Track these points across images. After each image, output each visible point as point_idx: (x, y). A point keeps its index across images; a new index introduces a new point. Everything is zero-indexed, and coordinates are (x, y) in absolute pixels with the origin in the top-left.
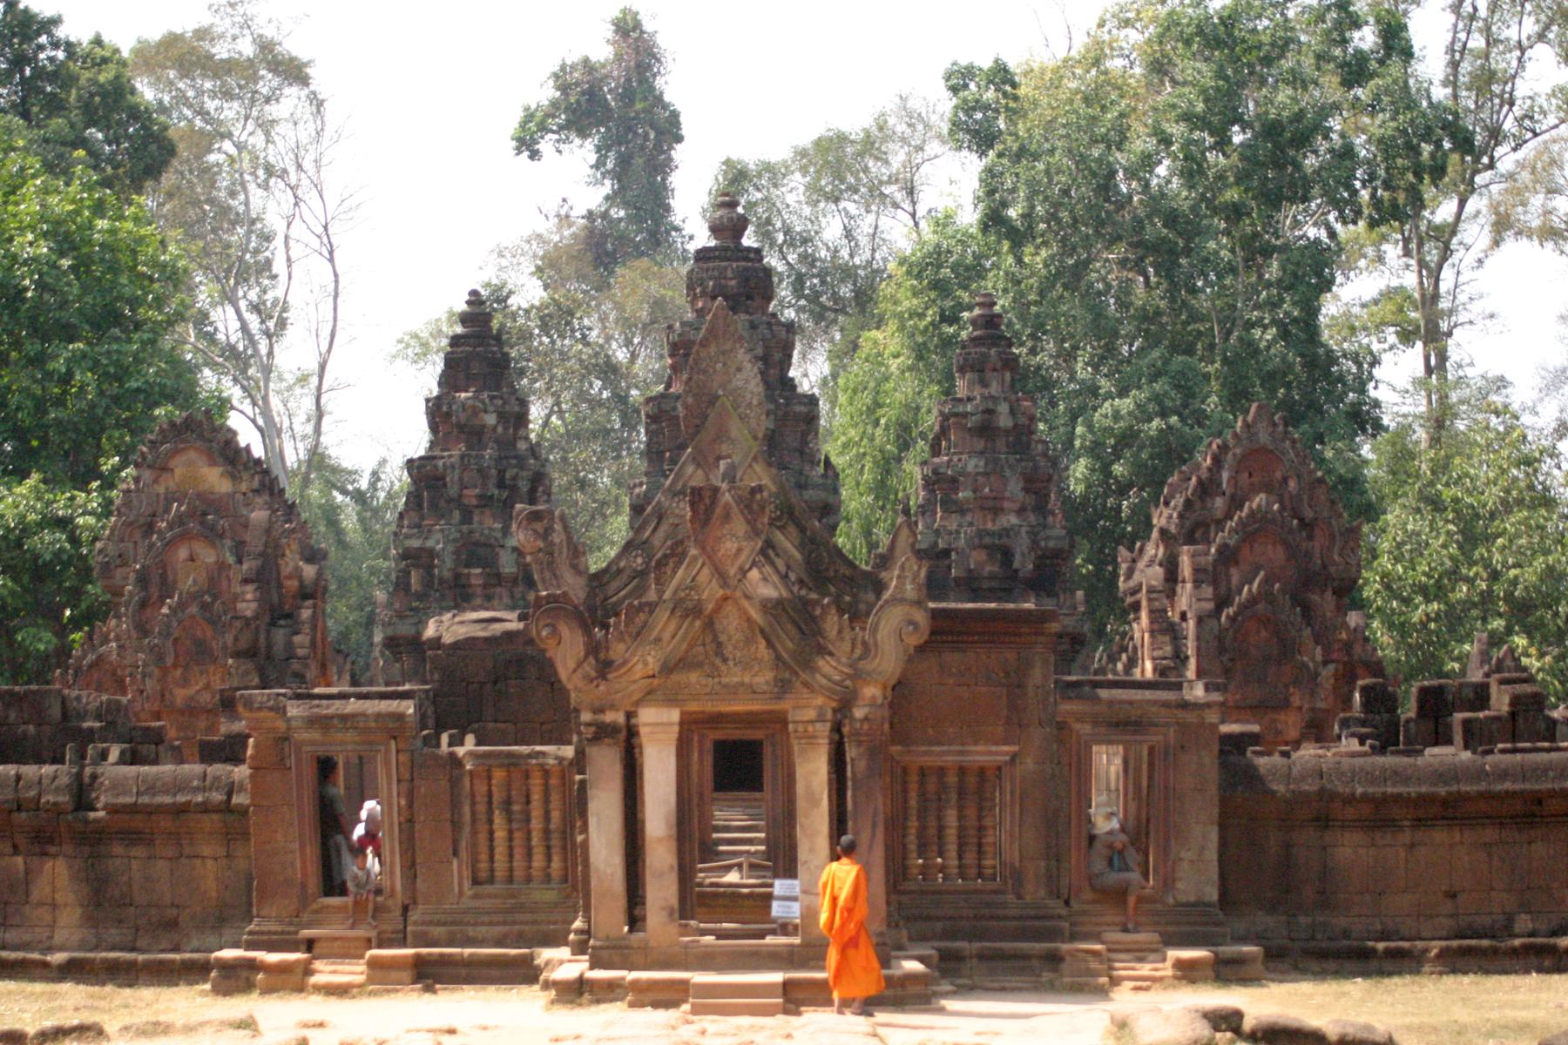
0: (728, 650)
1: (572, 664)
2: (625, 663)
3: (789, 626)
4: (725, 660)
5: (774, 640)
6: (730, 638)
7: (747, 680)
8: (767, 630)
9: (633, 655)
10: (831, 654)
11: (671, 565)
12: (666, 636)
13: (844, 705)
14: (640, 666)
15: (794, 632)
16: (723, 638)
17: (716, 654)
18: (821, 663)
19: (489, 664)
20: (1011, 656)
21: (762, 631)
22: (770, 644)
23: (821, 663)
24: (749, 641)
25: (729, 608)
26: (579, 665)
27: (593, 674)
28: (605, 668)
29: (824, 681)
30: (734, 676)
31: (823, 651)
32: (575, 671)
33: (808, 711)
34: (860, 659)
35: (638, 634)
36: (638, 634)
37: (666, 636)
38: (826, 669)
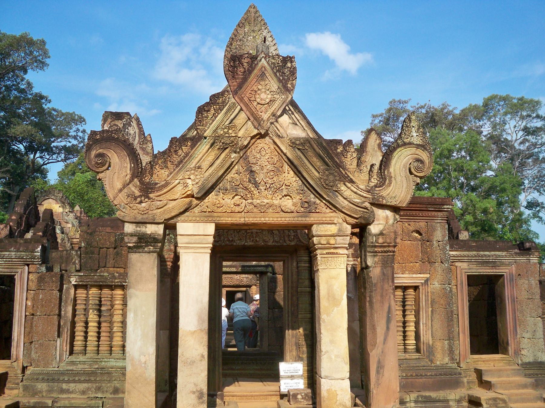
1: (119, 185)
2: (167, 184)
3: (315, 159)
4: (256, 185)
5: (301, 169)
6: (262, 168)
7: (276, 202)
8: (296, 162)
10: (352, 181)
11: (212, 111)
12: (205, 165)
15: (318, 163)
16: (255, 168)
17: (250, 181)
18: (343, 188)
19: (113, 239)
20: (421, 225)
21: (291, 163)
22: (298, 173)
23: (343, 188)
24: (278, 171)
27: (137, 193)
28: (147, 189)
29: (346, 203)
30: (263, 198)
32: (121, 190)
33: (331, 230)
34: (376, 186)
35: (181, 161)
36: (181, 161)
37: (205, 165)
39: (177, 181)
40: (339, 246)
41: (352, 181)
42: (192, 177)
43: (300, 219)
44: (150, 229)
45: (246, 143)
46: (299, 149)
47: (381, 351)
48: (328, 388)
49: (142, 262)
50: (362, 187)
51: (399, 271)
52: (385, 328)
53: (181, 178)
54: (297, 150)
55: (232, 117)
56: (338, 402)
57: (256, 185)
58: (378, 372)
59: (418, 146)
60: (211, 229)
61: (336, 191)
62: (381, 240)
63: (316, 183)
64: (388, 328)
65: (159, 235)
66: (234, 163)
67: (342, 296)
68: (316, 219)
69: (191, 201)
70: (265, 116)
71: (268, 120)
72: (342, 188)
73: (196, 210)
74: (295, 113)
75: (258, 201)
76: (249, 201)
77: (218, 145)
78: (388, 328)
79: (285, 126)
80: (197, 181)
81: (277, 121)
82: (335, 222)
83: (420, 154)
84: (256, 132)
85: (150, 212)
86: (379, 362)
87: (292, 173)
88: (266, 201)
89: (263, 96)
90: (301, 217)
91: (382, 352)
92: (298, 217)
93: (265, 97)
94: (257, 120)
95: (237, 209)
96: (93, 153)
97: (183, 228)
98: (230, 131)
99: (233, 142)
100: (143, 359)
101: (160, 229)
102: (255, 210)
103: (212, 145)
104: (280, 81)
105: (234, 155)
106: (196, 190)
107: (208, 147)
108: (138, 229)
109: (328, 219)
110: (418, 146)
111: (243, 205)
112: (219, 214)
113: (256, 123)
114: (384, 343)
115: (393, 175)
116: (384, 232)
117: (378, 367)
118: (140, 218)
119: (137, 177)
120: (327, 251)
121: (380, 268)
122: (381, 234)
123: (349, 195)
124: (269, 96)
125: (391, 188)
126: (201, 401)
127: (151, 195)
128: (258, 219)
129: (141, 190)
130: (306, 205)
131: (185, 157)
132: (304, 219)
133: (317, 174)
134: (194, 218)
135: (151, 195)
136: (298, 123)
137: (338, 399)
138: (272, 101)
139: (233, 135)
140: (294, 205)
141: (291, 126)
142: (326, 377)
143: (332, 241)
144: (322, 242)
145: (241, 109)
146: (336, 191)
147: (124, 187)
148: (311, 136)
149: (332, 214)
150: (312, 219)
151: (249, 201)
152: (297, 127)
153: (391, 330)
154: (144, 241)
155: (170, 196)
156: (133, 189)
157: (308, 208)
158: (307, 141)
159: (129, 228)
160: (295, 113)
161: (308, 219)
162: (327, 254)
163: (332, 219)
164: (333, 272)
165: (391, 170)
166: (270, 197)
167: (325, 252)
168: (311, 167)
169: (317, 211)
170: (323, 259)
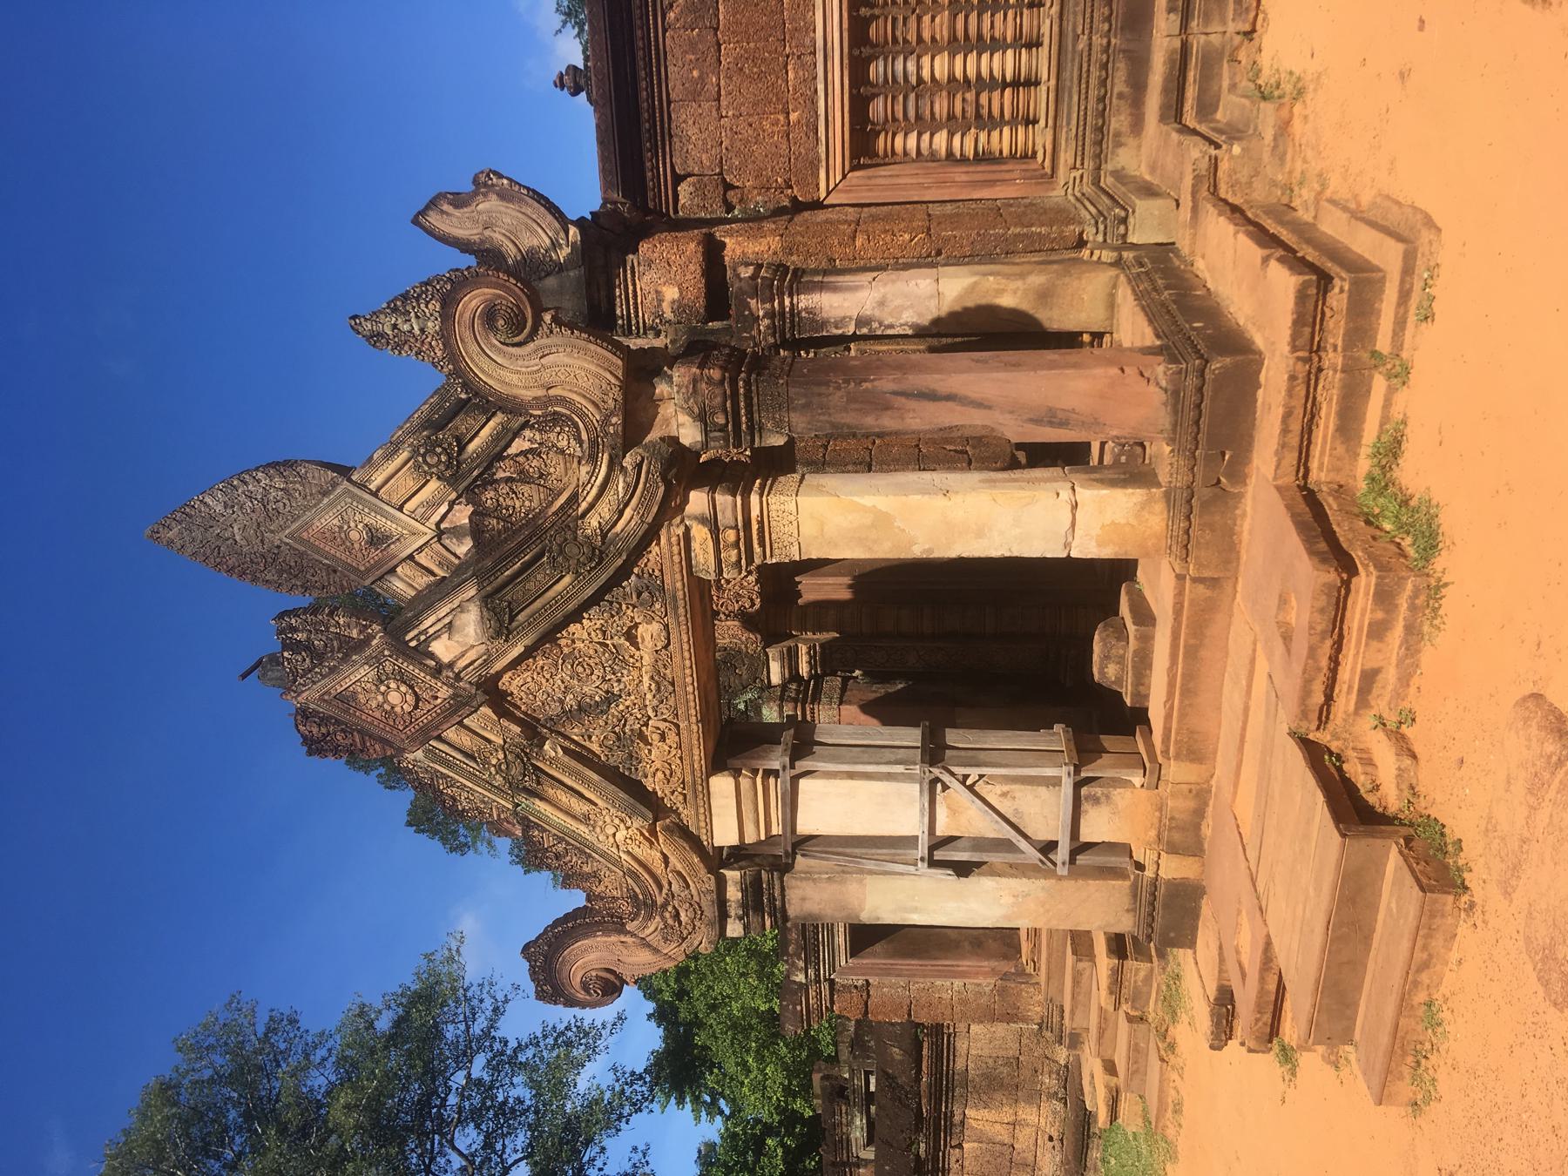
0: (592, 689)
3: (531, 585)
4: (610, 698)
7: (647, 660)
8: (543, 626)
9: (617, 863)
10: (574, 499)
12: (579, 807)
13: (684, 470)
14: (637, 851)
18: (593, 521)
23: (593, 521)
25: (512, 684)
26: (645, 944)
29: (628, 512)
31: (570, 516)
32: (656, 951)
38: (604, 510)
39: (624, 856)
40: (740, 518)
41: (574, 499)
42: (610, 830)
43: (681, 611)
44: (733, 894)
45: (516, 729)
46: (512, 619)
47: (1008, 416)
48: (1094, 543)
49: (803, 899)
50: (584, 477)
51: (807, 41)
52: (950, 404)
53: (614, 850)
54: (514, 624)
55: (459, 756)
56: (1134, 522)
57: (610, 698)
58: (1063, 424)
59: (447, 316)
60: (722, 785)
61: (604, 536)
62: (720, 420)
63: (589, 582)
64: (950, 398)
65: (743, 877)
66: (567, 744)
67: (864, 509)
68: (678, 576)
69: (666, 829)
70: (444, 692)
71: (451, 686)
72: (595, 523)
73: (687, 814)
74: (422, 627)
75: (649, 696)
76: (651, 714)
77: (529, 783)
78: (950, 398)
79: (458, 650)
80: (617, 821)
81: (451, 665)
82: (680, 531)
83: (467, 315)
84: (485, 710)
85: (696, 898)
86: (1037, 421)
87: (572, 628)
88: (646, 679)
89: (394, 698)
90: (676, 608)
91: (1011, 412)
92: (677, 616)
93: (397, 697)
94: (459, 707)
95: (672, 738)
96: (581, 995)
97: (725, 834)
98: (494, 762)
99: (518, 756)
100: (1007, 900)
101: (732, 875)
102: (671, 702)
103: (532, 793)
104: (346, 658)
105: (547, 747)
106: (637, 823)
107: (537, 802)
108: (733, 913)
109: (675, 549)
110: (447, 316)
111: (662, 725)
112: (688, 770)
113: (467, 710)
114: (990, 408)
115: (540, 393)
116: (696, 410)
117: (1051, 424)
118: (710, 912)
119: (623, 925)
120: (756, 545)
121: (792, 415)
122: (702, 418)
123: (609, 504)
124: (393, 685)
125: (575, 397)
126: (1103, 799)
127: (660, 900)
128: (691, 697)
129: (650, 917)
130: (645, 595)
131: (568, 844)
132: (681, 603)
133: (567, 580)
134: (702, 817)
135: (660, 900)
136: (447, 620)
137: (1123, 521)
138: (402, 678)
139: (501, 756)
140: (650, 620)
141: (457, 637)
142: (1067, 545)
143: (730, 536)
144: (734, 559)
145: (439, 738)
146: (604, 536)
147: (649, 946)
148: (472, 592)
149: (663, 541)
150: (679, 585)
151: (651, 714)
152: (457, 623)
153: (954, 391)
154: (757, 900)
155: (658, 867)
156: (648, 931)
157: (653, 590)
158: (488, 601)
159: (734, 929)
160: (422, 627)
161: (680, 594)
162: (762, 544)
163: (674, 540)
164: (808, 529)
165: (528, 395)
166: (635, 674)
167: (757, 549)
168: (551, 594)
169: (657, 573)
170: (776, 552)
